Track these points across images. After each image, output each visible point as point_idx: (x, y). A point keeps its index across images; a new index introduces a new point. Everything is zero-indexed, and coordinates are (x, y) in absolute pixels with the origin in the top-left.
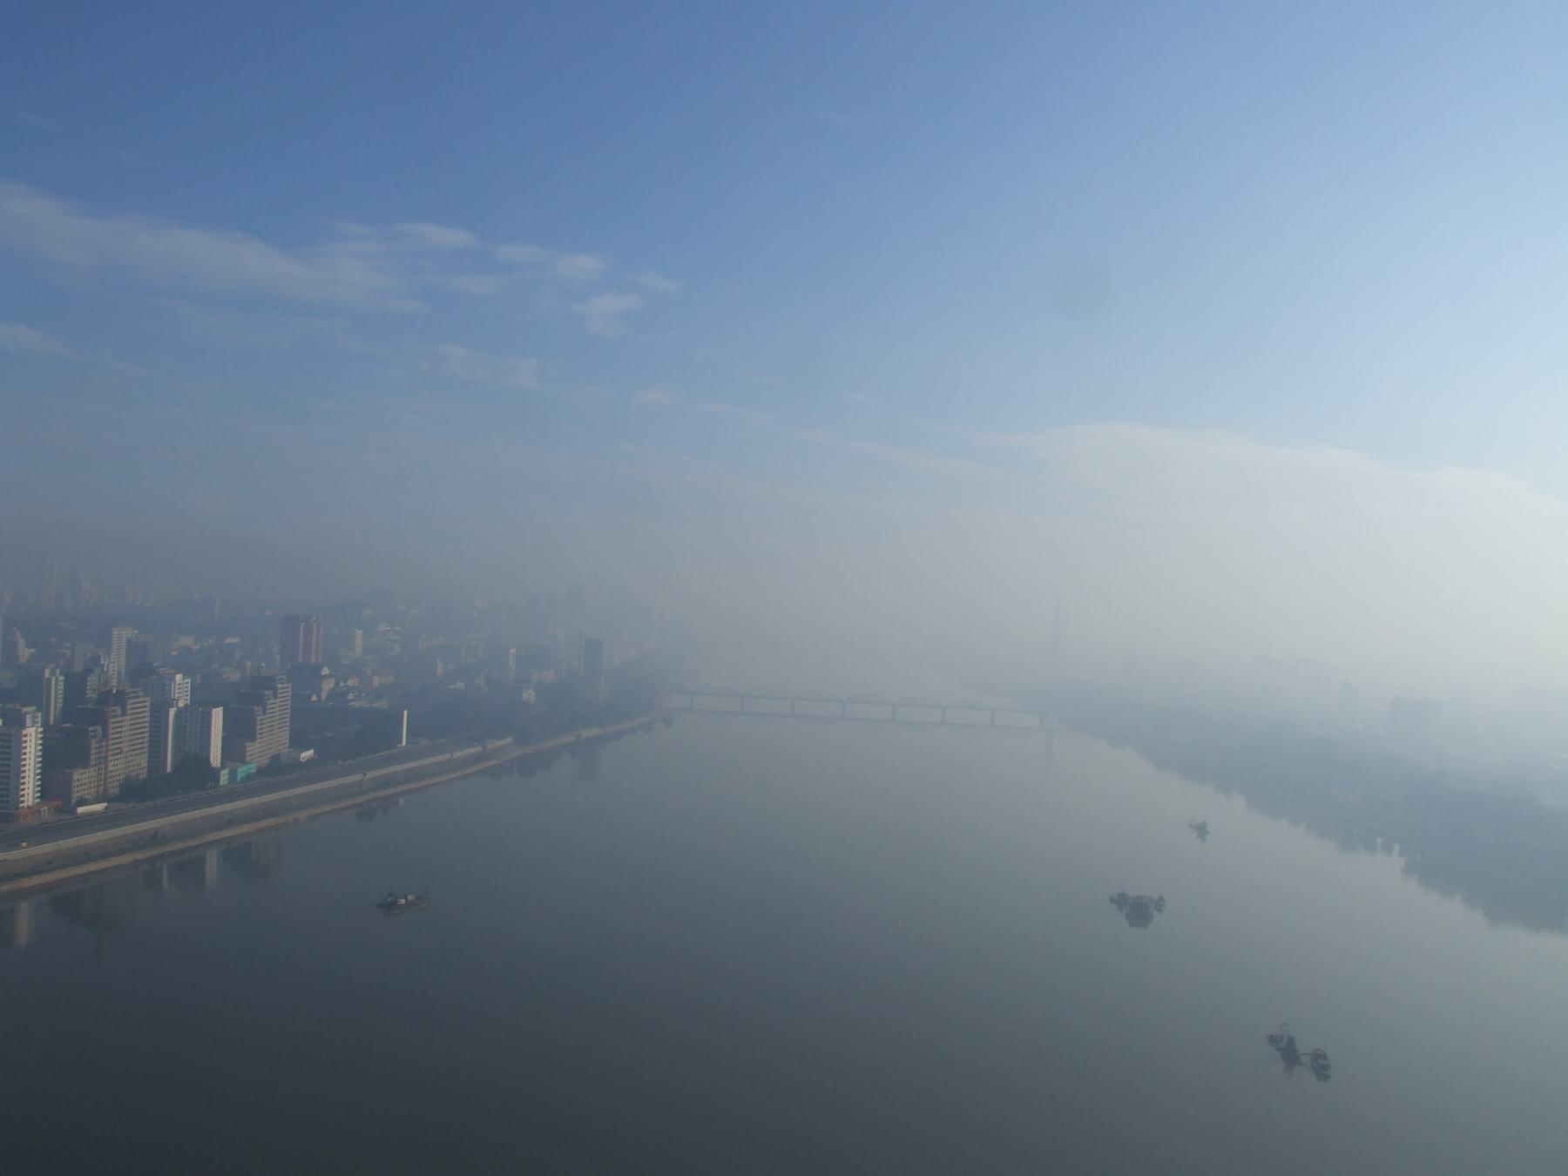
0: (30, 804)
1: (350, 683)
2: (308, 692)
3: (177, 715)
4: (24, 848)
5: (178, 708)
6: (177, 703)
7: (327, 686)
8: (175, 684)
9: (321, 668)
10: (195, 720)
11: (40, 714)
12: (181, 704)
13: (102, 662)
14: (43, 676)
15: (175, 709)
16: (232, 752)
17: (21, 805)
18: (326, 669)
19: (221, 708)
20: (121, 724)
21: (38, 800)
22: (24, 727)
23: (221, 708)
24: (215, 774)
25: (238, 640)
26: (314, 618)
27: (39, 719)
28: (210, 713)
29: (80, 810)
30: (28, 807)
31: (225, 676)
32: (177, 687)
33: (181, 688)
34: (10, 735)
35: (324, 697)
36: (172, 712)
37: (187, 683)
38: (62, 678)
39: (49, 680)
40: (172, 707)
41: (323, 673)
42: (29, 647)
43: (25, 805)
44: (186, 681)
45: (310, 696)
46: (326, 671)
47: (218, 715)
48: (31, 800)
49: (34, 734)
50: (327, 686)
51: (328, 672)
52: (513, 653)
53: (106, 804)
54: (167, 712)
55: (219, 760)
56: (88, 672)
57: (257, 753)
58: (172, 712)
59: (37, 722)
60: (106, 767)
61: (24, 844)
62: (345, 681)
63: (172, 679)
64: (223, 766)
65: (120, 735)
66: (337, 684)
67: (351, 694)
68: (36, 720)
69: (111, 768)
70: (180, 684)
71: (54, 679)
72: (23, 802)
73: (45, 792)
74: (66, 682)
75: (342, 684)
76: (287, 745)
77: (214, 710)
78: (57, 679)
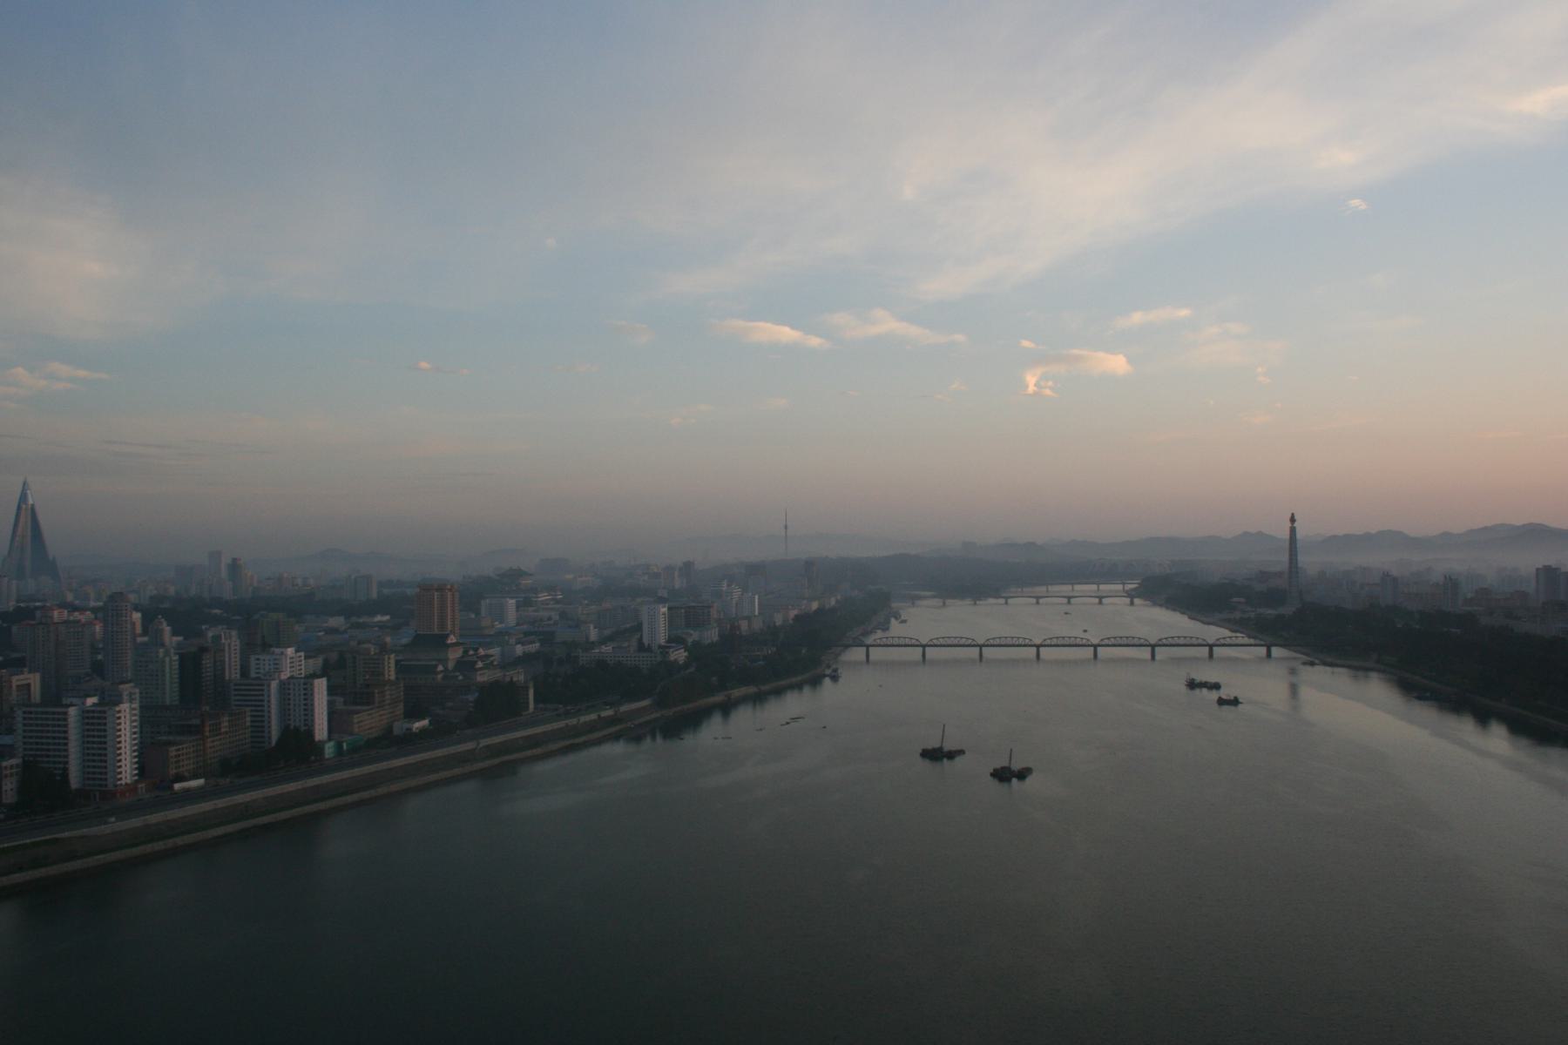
0: (129, 781)
2: (434, 663)
4: (114, 823)
7: (454, 655)
11: (137, 691)
12: (284, 676)
15: (277, 681)
17: (119, 782)
18: (452, 637)
21: (136, 778)
24: (318, 748)
27: (137, 696)
28: (312, 684)
29: (177, 786)
30: (126, 784)
32: (288, 661)
35: (451, 665)
36: (274, 685)
37: (300, 657)
40: (274, 679)
41: (449, 642)
43: (123, 782)
44: (299, 654)
48: (128, 778)
49: (128, 710)
51: (454, 641)
52: (664, 614)
54: (269, 686)
57: (368, 722)
58: (274, 685)
59: (135, 699)
61: (113, 819)
64: (330, 739)
66: (466, 652)
68: (133, 697)
70: (291, 658)
72: (121, 779)
73: (142, 770)
75: (471, 652)
76: (402, 716)
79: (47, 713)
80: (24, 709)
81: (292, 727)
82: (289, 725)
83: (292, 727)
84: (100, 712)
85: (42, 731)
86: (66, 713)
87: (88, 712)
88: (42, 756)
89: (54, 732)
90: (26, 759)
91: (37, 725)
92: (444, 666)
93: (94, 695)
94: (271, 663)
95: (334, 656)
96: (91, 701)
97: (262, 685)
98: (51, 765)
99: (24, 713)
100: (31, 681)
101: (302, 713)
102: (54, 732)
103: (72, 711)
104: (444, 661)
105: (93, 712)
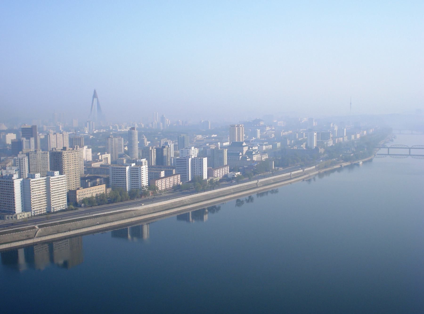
1: (254, 148)
3: (191, 160)
4: (143, 206)
5: (192, 158)
6: (191, 156)
7: (245, 149)
8: (191, 150)
9: (242, 143)
10: (197, 163)
12: (193, 157)
13: (168, 144)
14: (149, 149)
15: (191, 159)
16: (210, 173)
19: (207, 158)
22: (142, 165)
23: (207, 158)
26: (241, 125)
27: (147, 163)
28: (202, 160)
31: (211, 148)
32: (192, 151)
33: (194, 152)
34: (138, 168)
36: (190, 159)
37: (196, 150)
38: (155, 150)
39: (151, 151)
40: (190, 158)
41: (243, 145)
42: (148, 141)
44: (195, 149)
45: (240, 153)
46: (244, 144)
47: (205, 160)
50: (245, 149)
51: (245, 145)
52: (315, 135)
54: (188, 160)
55: (207, 177)
56: (164, 147)
57: (219, 174)
58: (190, 159)
59: (146, 164)
61: (143, 205)
62: (252, 148)
63: (190, 149)
66: (249, 148)
67: (254, 152)
71: (153, 150)
74: (156, 151)
75: (251, 149)
77: (204, 159)
78: (154, 150)
84: (136, 168)
86: (125, 169)
87: (132, 168)
92: (242, 153)
93: (134, 163)
96: (133, 165)
103: (128, 168)
104: (242, 152)
105: (134, 168)
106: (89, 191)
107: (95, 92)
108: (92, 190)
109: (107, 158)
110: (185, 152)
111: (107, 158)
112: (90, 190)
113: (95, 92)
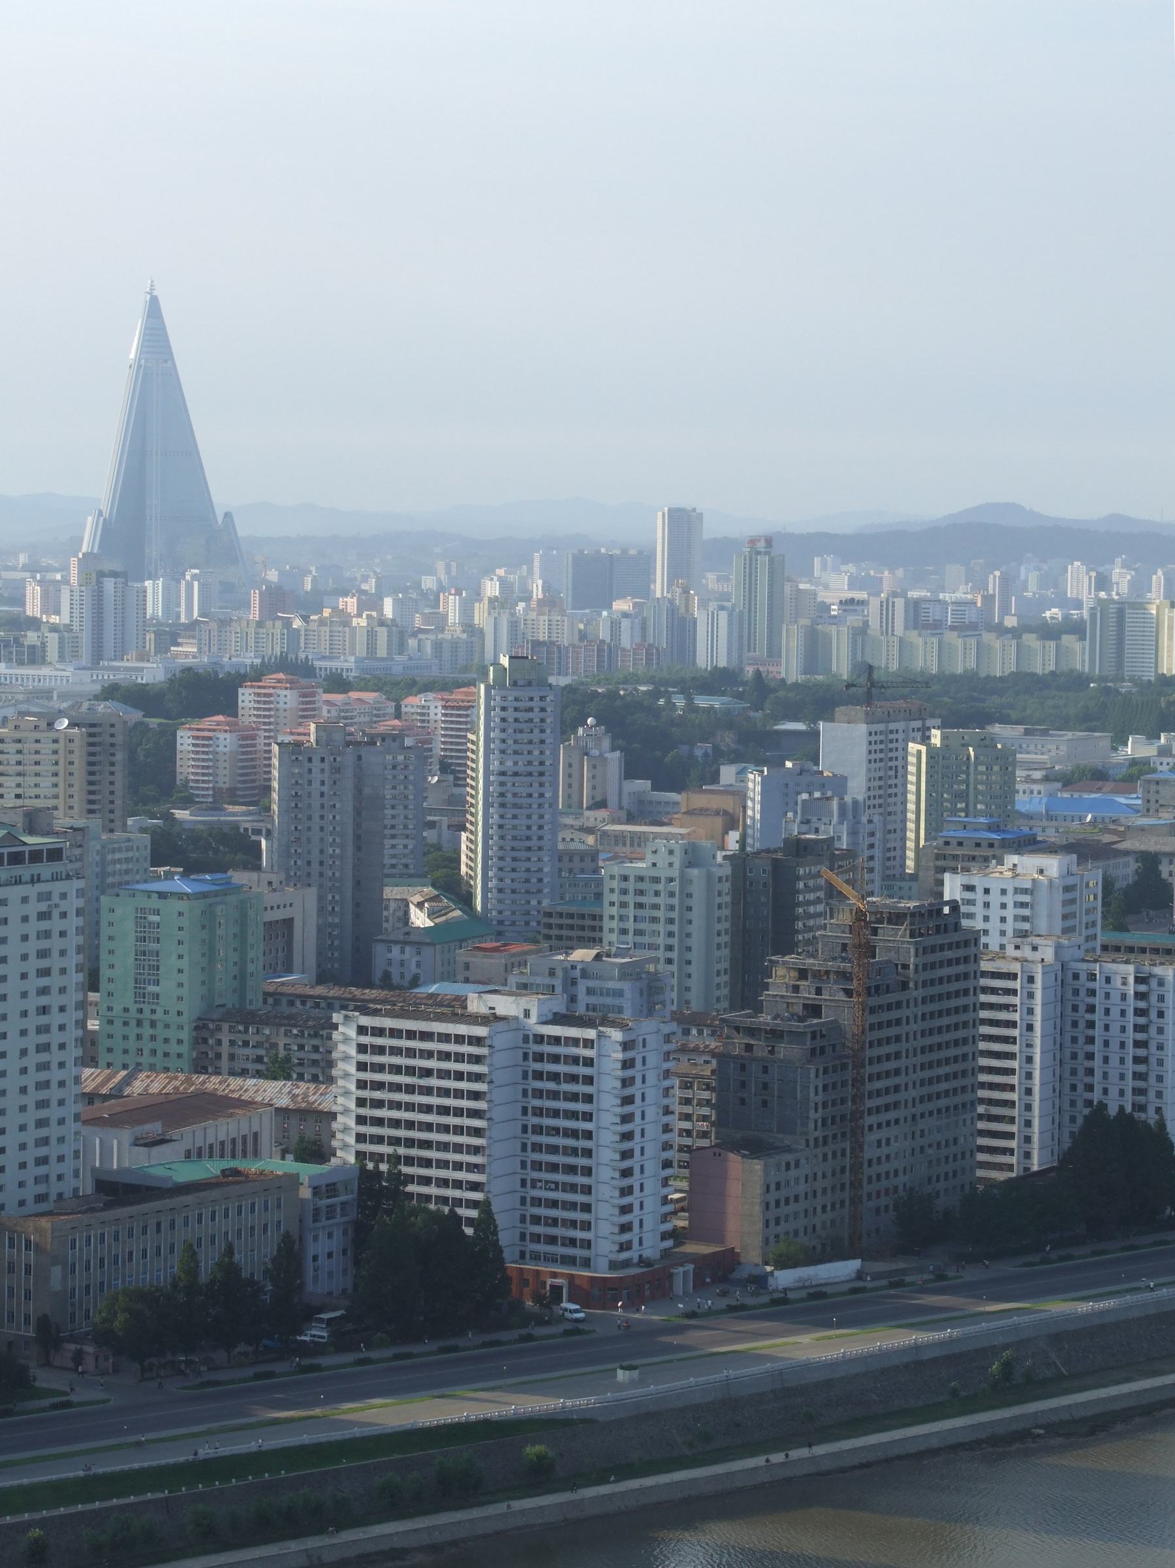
0: (648, 1253)
20: (894, 1015)
25: (479, 908)
53: (854, 1265)
60: (858, 1147)
65: (892, 1048)
69: (869, 1153)
79: (426, 1036)
80: (366, 1021)
81: (1113, 1111)
82: (1103, 1106)
83: (1113, 1111)
85: (410, 1089)
88: (409, 1161)
89: (445, 1092)
90: (370, 1166)
91: (397, 1069)
94: (1009, 899)
95: (1126, 871)
97: (1014, 976)
98: (432, 1190)
99: (362, 1030)
100: (296, 913)
101: (1130, 1065)
102: (445, 1092)
106: (172, 1225)
107: (154, 310)
108: (179, 1222)
109: (289, 923)
110: (995, 898)
111: (289, 923)
112: (165, 1220)
113: (154, 310)
